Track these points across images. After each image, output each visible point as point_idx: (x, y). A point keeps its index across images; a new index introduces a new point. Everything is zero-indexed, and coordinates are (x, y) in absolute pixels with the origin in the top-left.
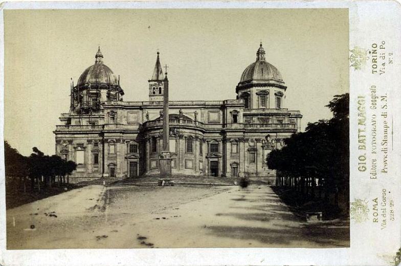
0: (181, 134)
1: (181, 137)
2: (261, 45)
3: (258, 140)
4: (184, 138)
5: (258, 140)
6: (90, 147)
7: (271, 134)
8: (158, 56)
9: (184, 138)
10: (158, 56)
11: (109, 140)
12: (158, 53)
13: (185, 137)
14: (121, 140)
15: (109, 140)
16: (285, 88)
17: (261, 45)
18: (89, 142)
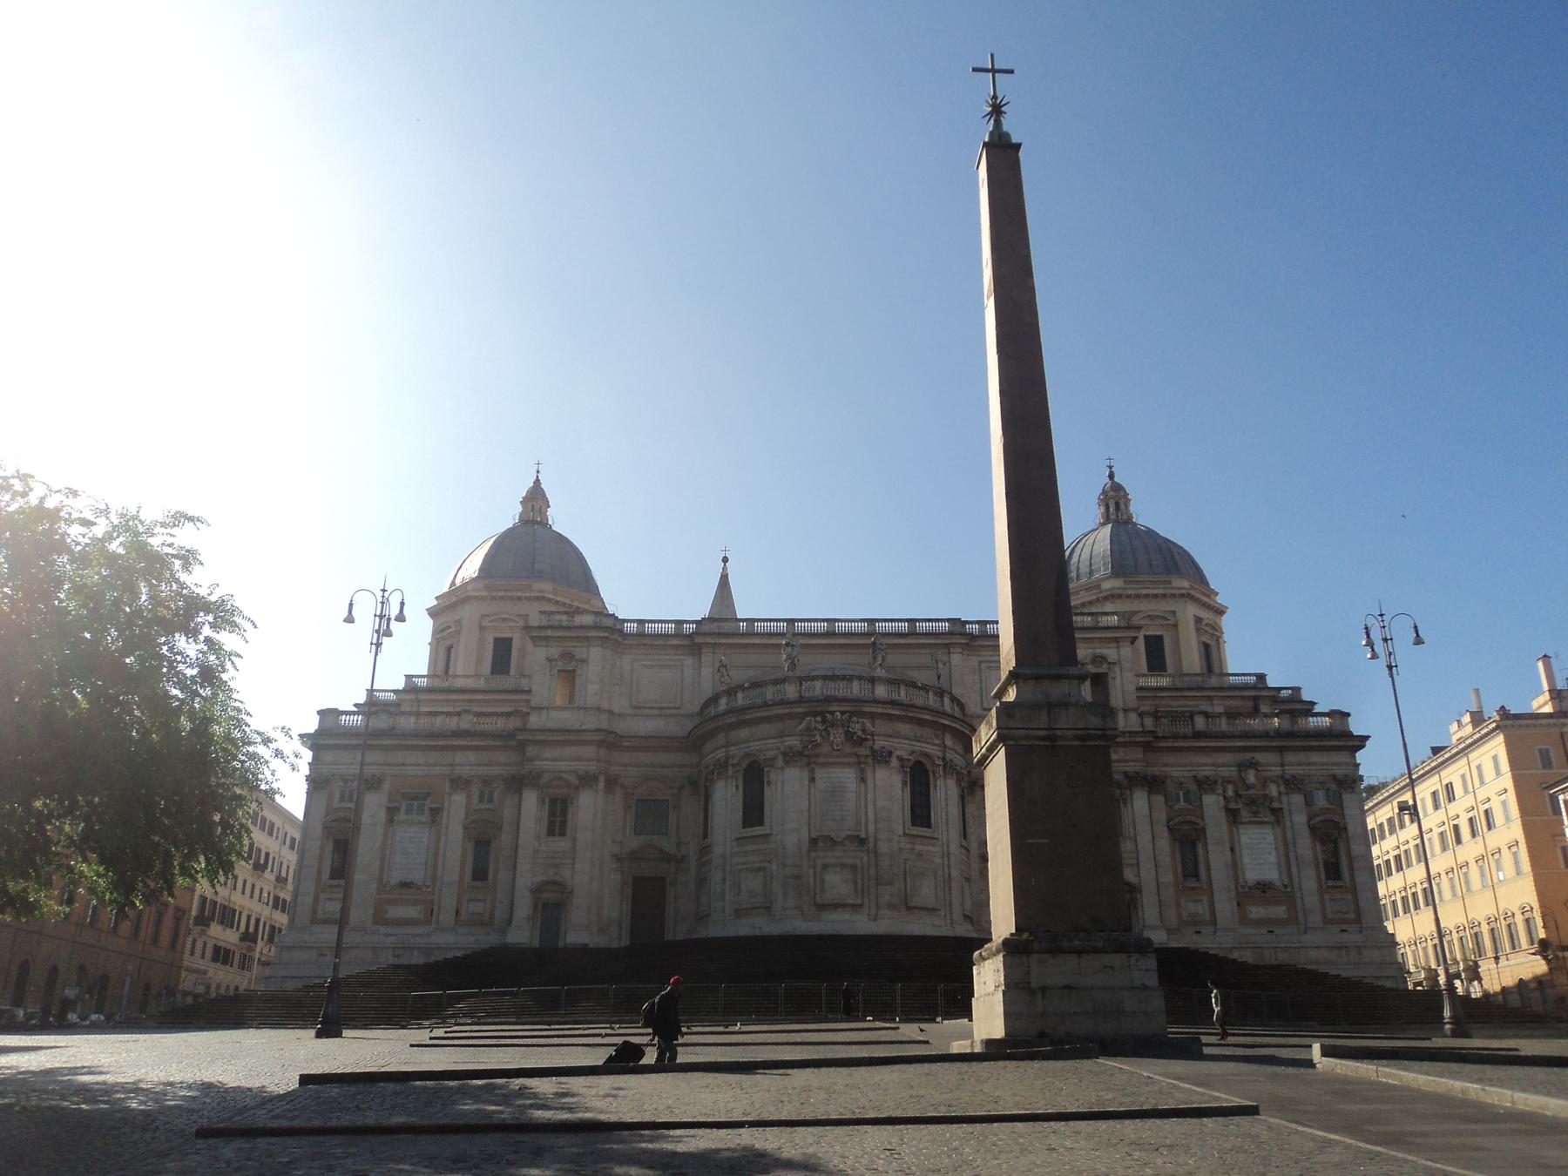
0: (880, 743)
1: (882, 757)
2: (1111, 476)
3: (1206, 785)
4: (894, 762)
5: (1206, 785)
6: (457, 807)
7: (1260, 757)
8: (724, 568)
9: (894, 762)
10: (724, 568)
11: (545, 778)
12: (725, 560)
13: (900, 759)
14: (602, 779)
15: (545, 778)
16: (1220, 612)
17: (1111, 476)
18: (459, 783)
